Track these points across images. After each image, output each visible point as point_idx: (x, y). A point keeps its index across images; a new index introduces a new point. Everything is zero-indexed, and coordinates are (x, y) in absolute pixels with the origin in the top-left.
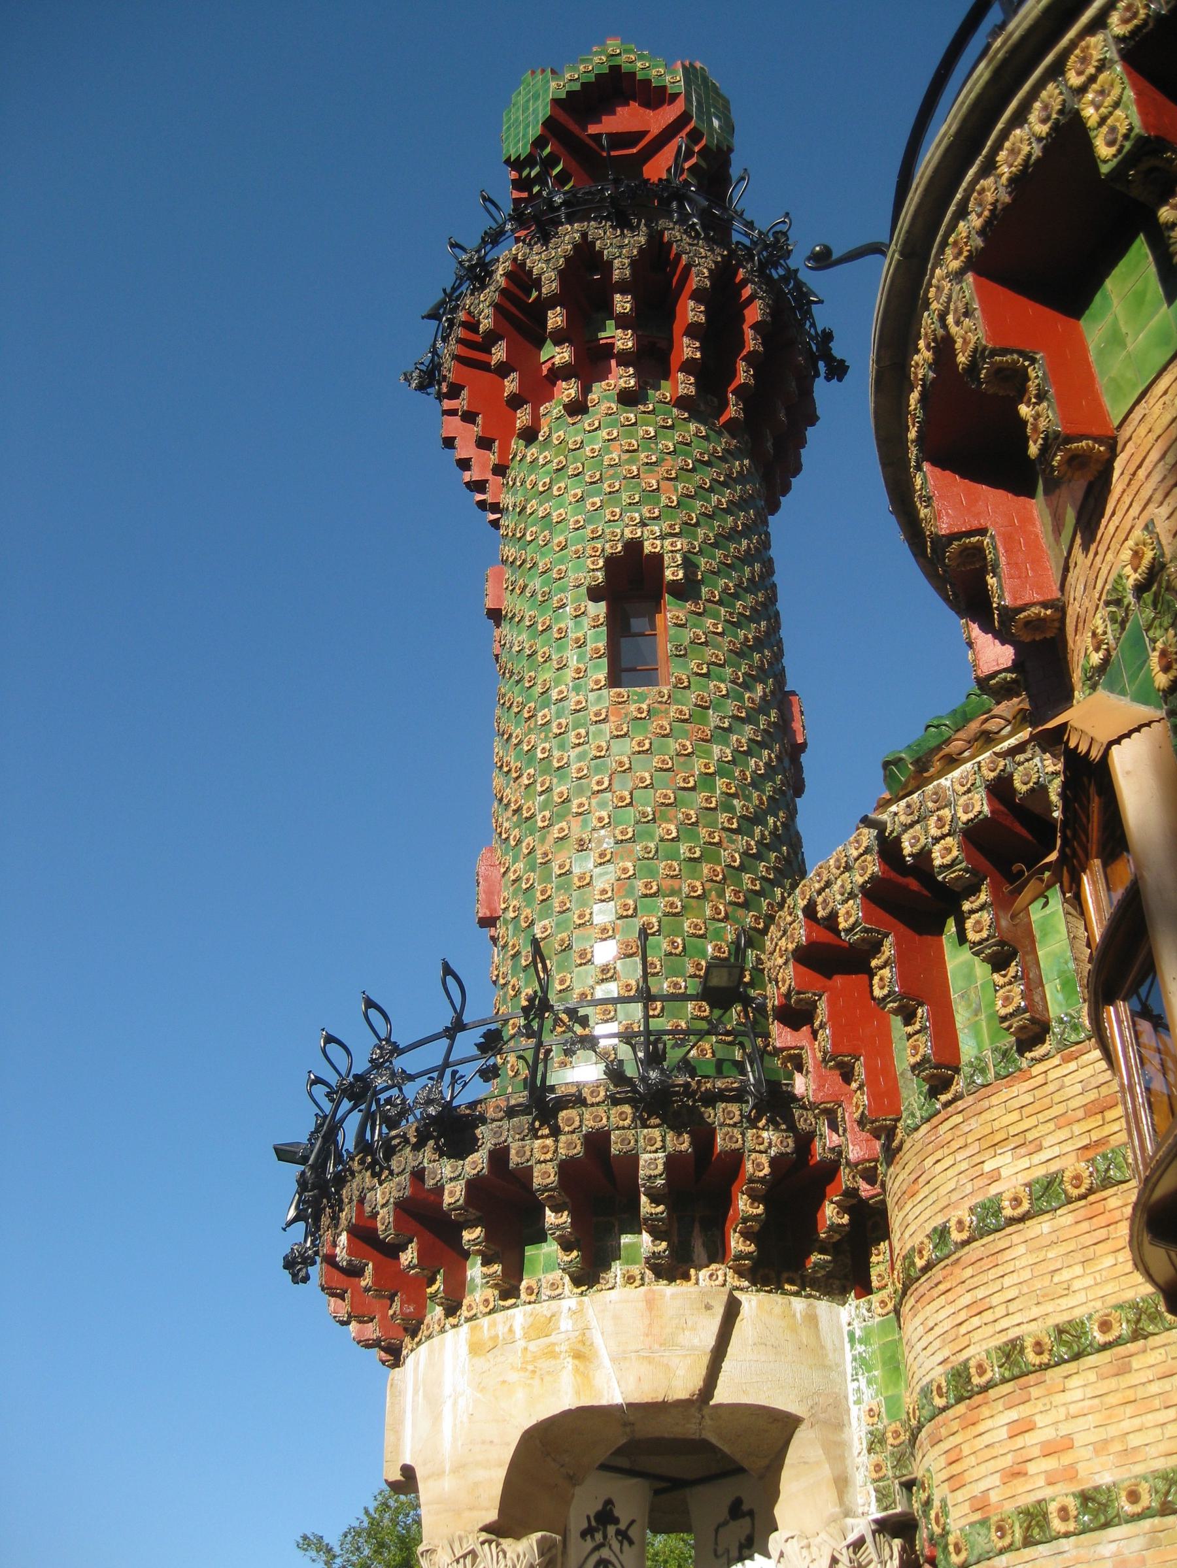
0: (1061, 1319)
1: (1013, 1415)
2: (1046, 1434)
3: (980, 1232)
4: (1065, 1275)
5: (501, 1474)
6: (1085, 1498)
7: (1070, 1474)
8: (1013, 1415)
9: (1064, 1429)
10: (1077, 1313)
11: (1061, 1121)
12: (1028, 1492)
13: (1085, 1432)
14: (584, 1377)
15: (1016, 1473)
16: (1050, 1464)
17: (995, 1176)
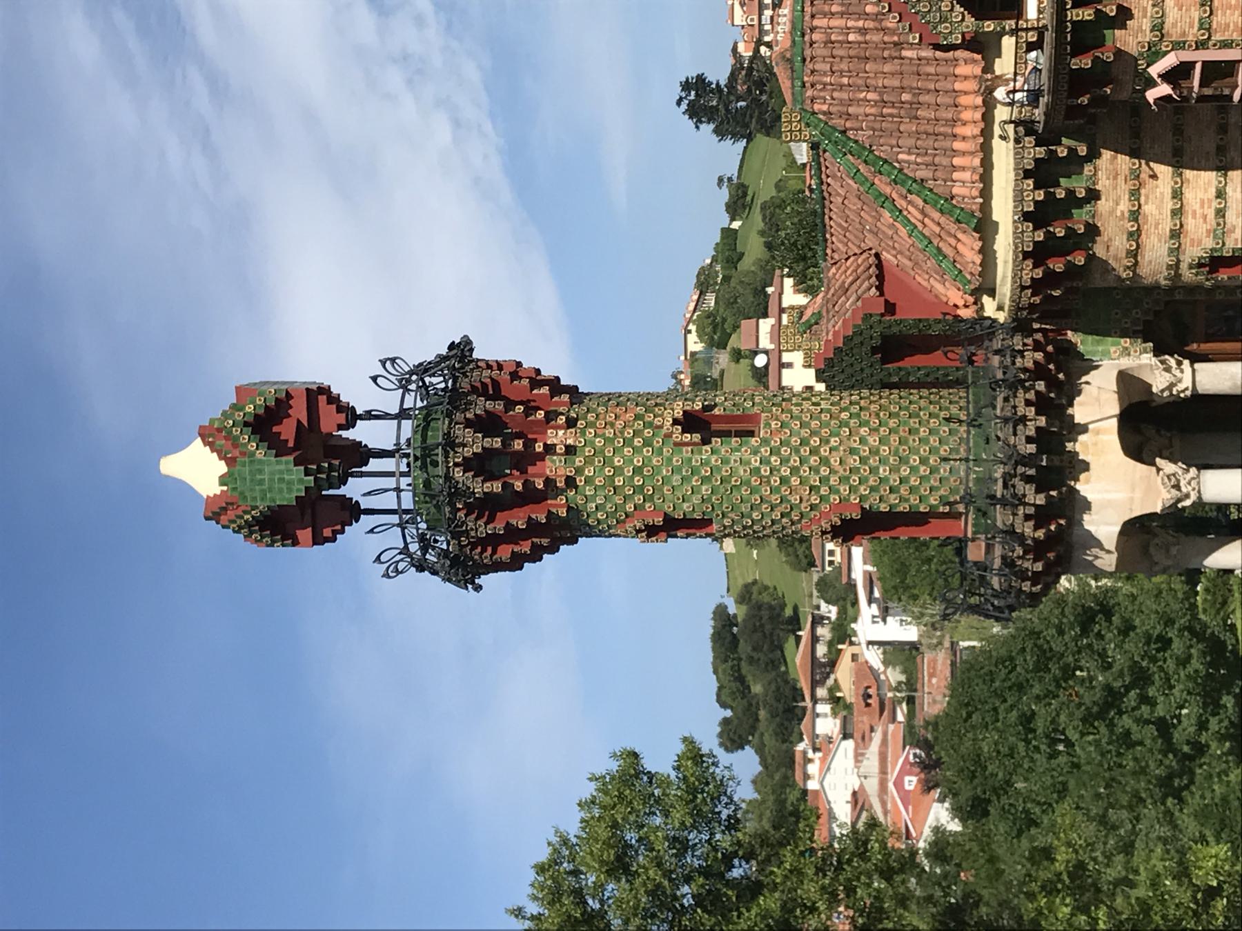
0: (1170, 196)
1: (1190, 216)
2: (1198, 205)
3: (1136, 220)
4: (1158, 194)
5: (1139, 465)
6: (1218, 197)
7: (1210, 201)
8: (1190, 216)
9: (1198, 200)
10: (1170, 191)
11: (1115, 188)
12: (1211, 214)
13: (1200, 195)
14: (1106, 431)
15: (1205, 217)
16: (1206, 206)
17: (1123, 213)
